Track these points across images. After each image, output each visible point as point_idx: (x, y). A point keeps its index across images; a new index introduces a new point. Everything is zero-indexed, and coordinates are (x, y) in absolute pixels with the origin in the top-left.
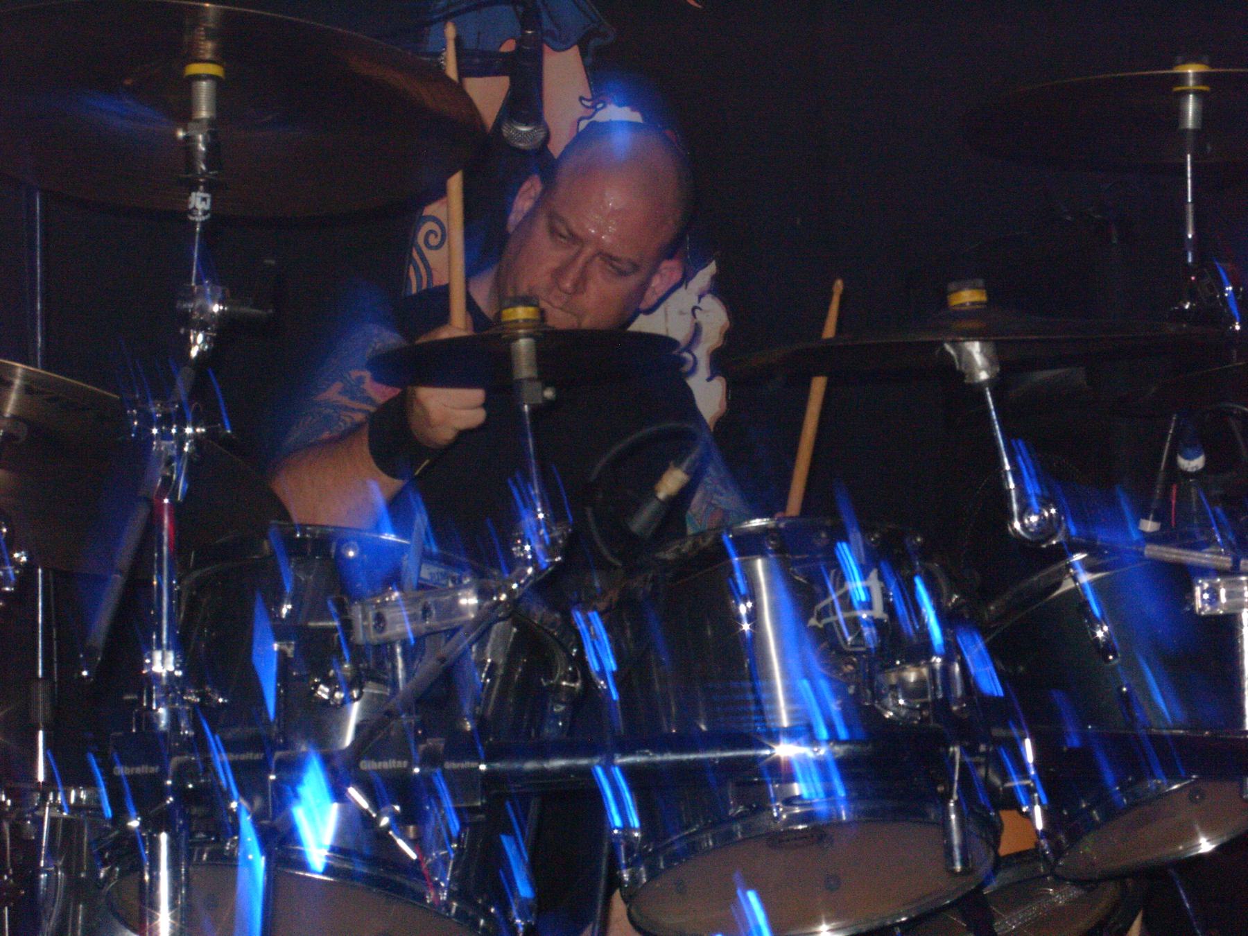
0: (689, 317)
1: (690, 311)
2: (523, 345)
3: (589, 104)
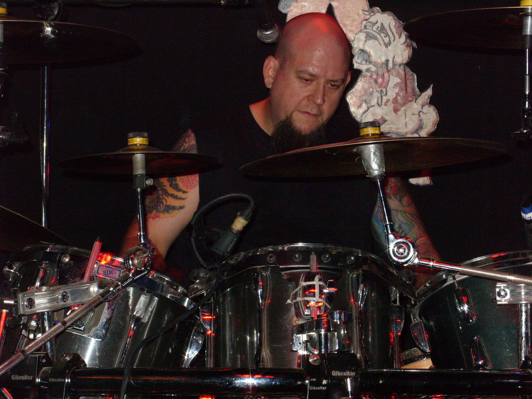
0: (417, 116)
1: (417, 113)
2: (139, 157)
3: (367, 13)
